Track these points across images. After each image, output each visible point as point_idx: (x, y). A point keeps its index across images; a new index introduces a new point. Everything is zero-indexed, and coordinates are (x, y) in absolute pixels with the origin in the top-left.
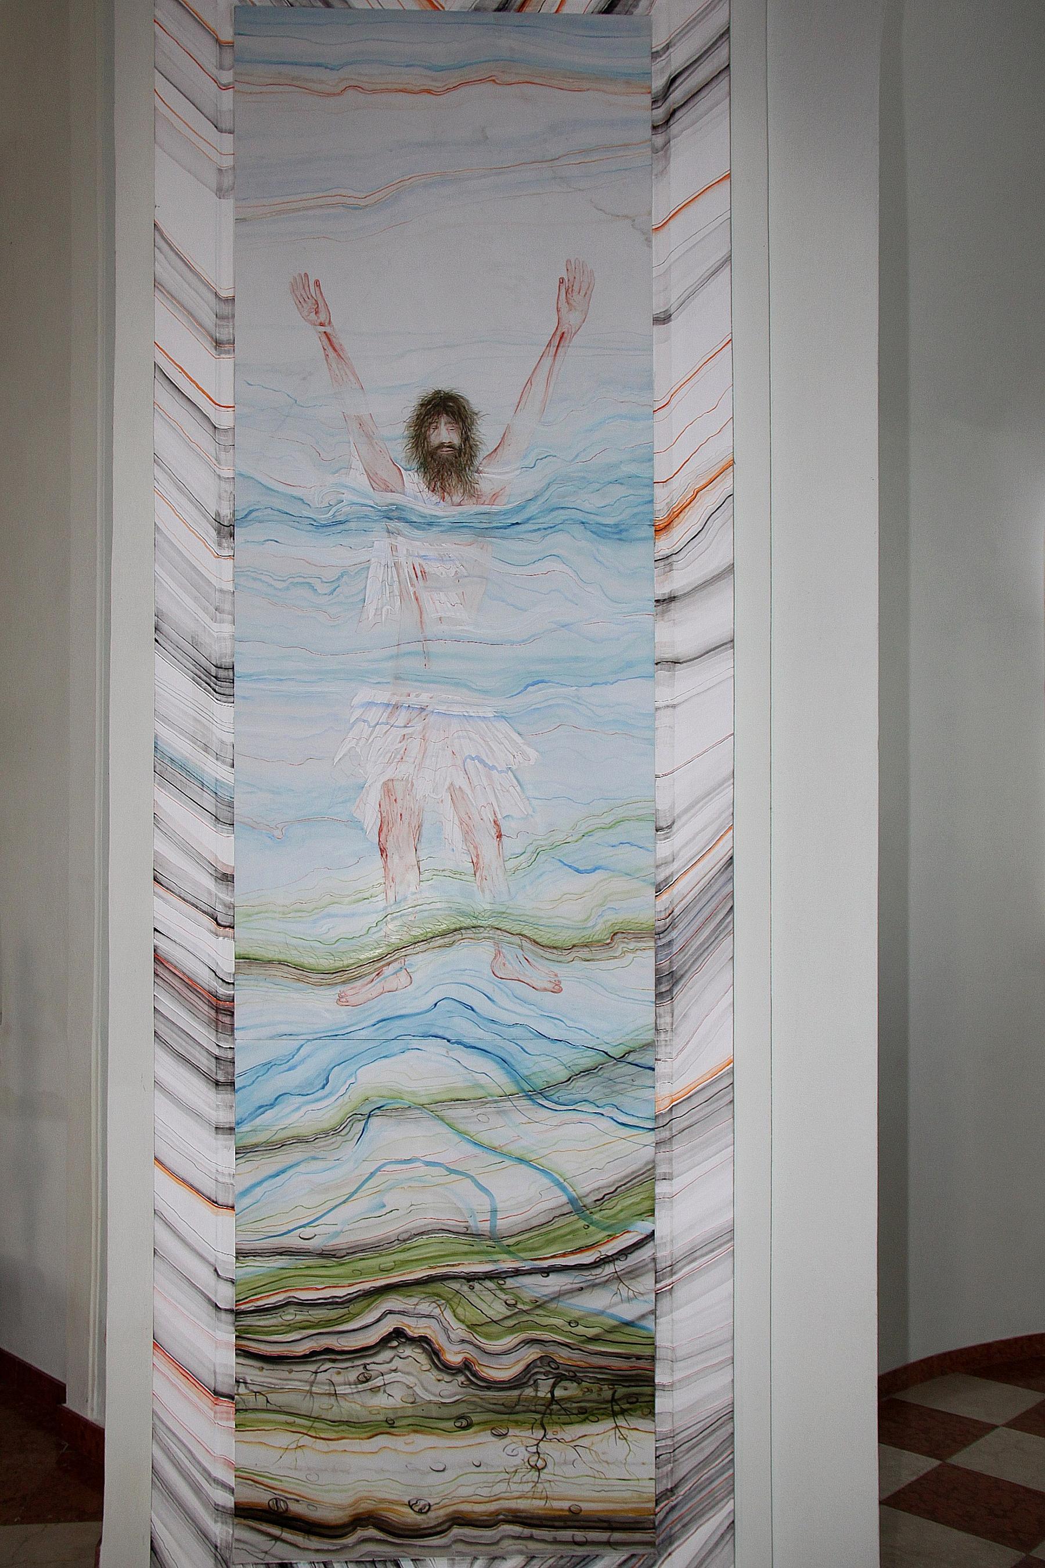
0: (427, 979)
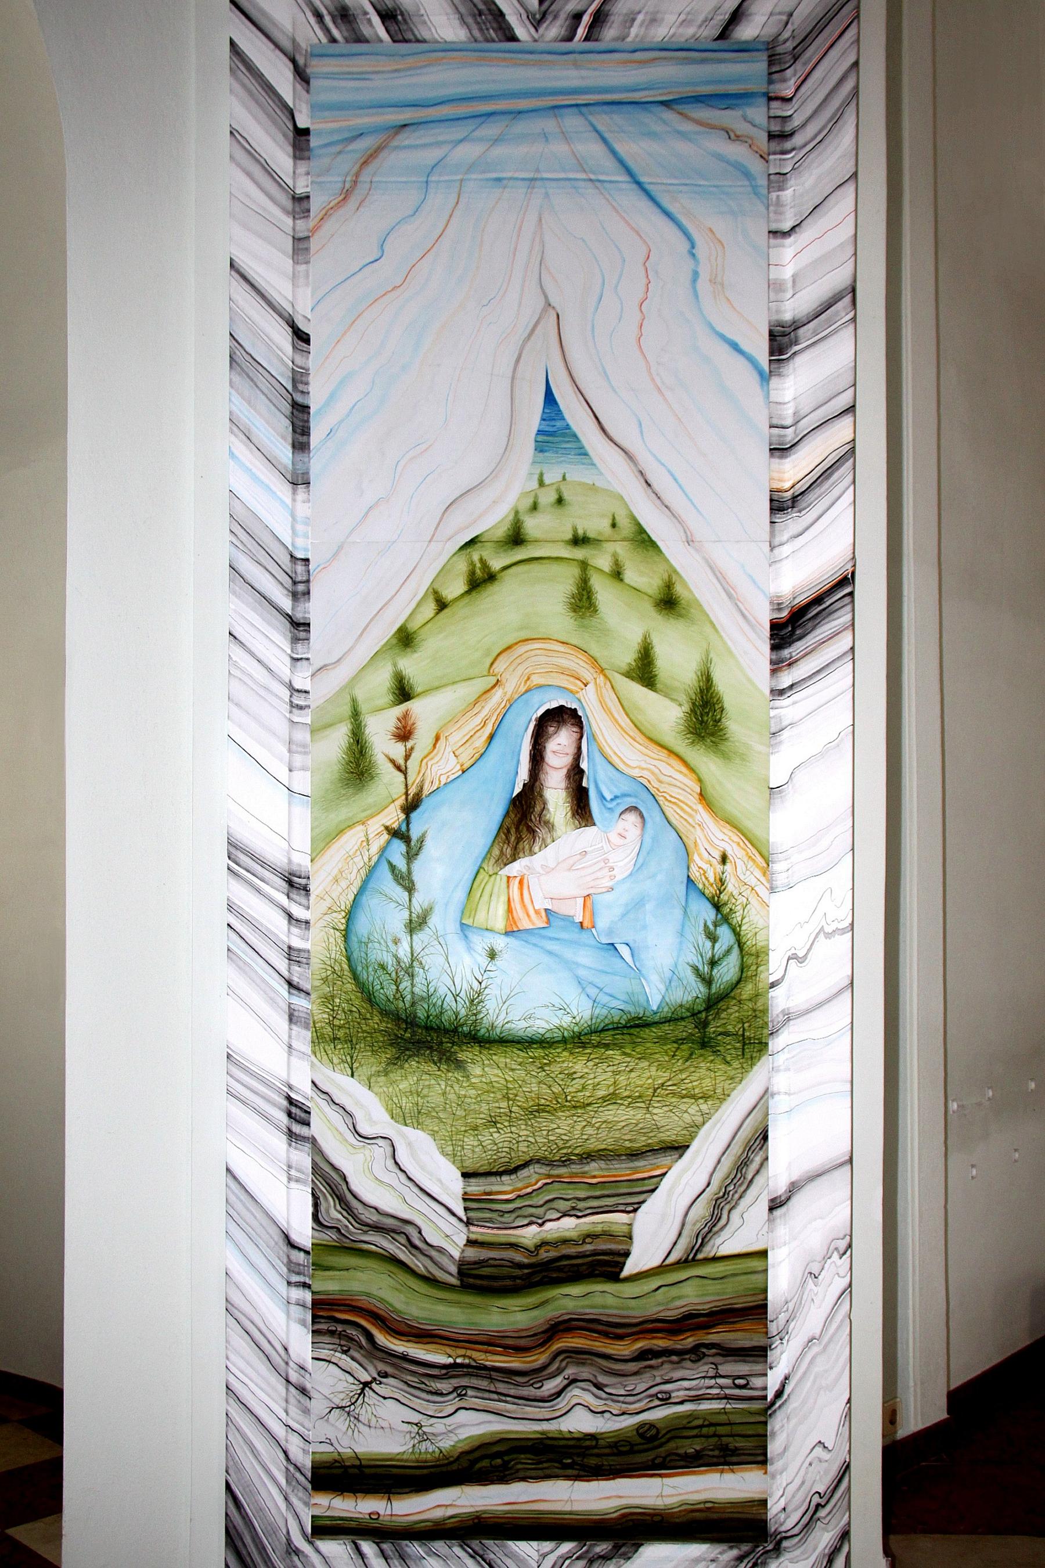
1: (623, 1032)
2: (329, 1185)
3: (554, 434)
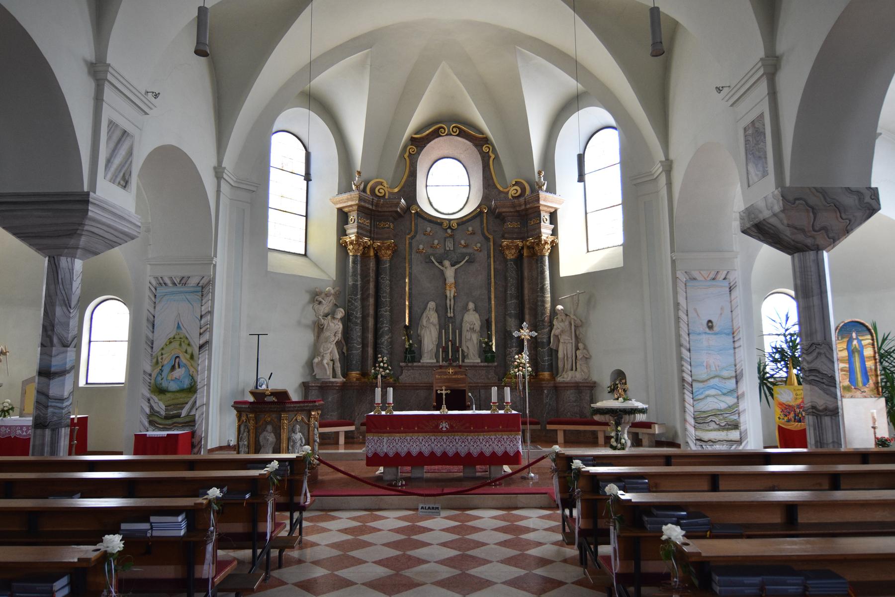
0: (713, 382)
1: (182, 390)
2: (151, 407)
3: (179, 327)
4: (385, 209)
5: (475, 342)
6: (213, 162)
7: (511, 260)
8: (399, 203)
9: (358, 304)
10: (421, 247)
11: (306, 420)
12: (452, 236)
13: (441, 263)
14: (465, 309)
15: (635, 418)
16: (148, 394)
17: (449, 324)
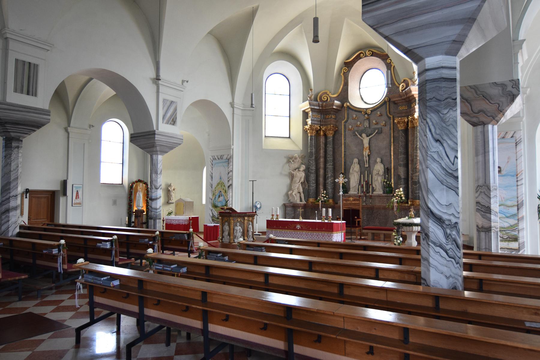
3: (221, 178)
4: (327, 108)
5: (380, 181)
6: (230, 100)
7: (402, 130)
8: (333, 105)
9: (313, 163)
10: (350, 127)
11: (242, 221)
12: (367, 118)
13: (361, 135)
14: (376, 162)
15: (413, 228)
16: (211, 208)
17: (366, 171)
